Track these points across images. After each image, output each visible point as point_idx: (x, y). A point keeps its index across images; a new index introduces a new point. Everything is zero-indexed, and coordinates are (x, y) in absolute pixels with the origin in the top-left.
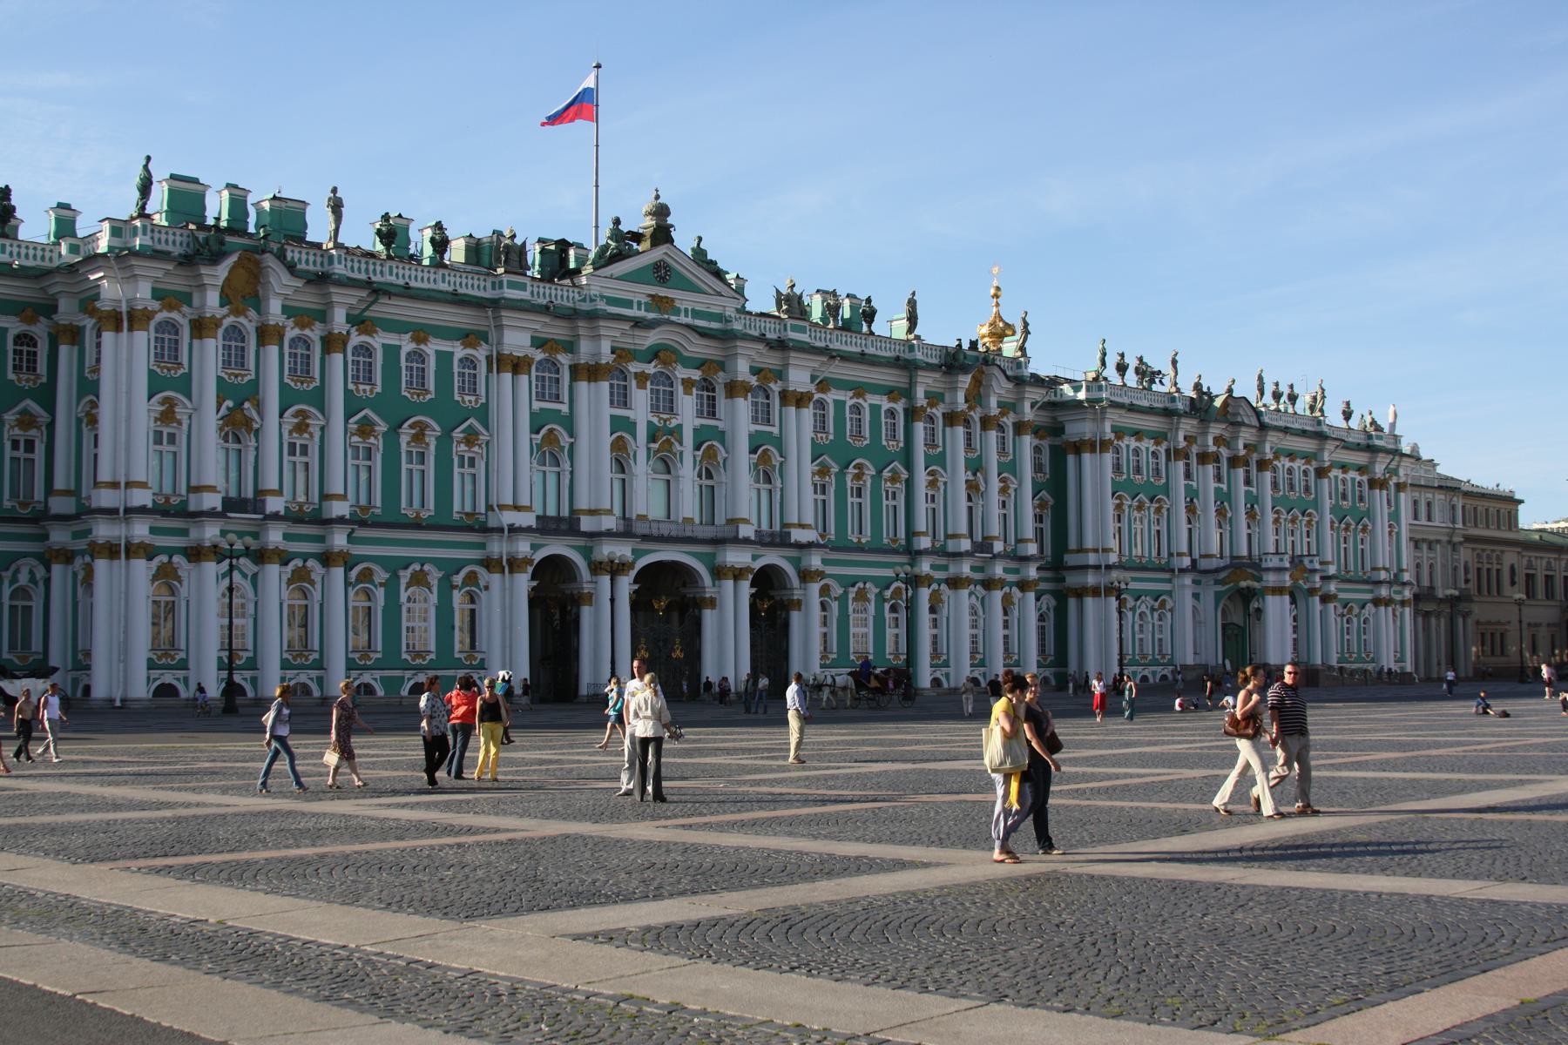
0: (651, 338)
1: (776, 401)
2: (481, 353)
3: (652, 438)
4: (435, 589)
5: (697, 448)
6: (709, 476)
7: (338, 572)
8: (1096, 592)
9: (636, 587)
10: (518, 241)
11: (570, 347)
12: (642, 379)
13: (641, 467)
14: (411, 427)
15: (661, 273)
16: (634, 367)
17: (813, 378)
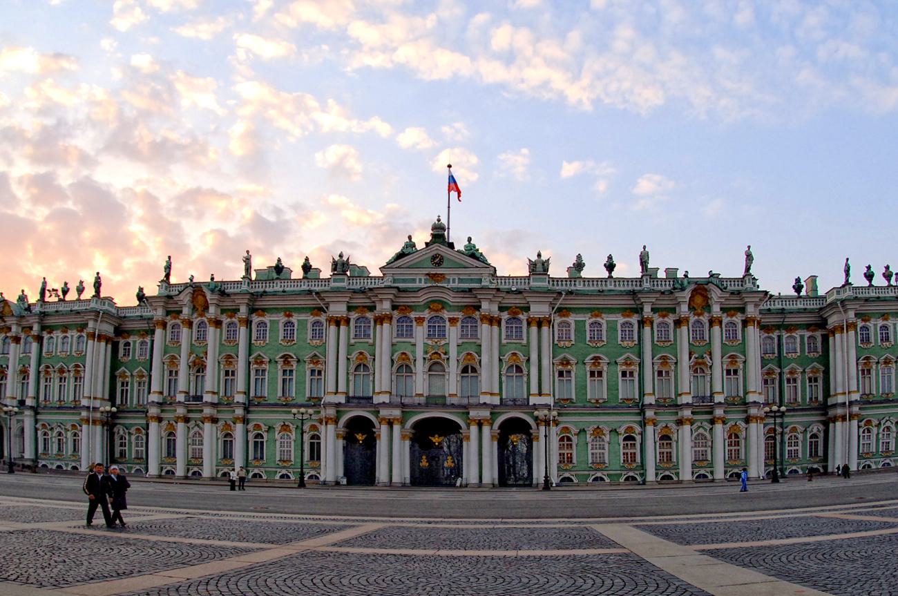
0: (422, 299)
1: (525, 323)
2: (323, 318)
3: (426, 352)
4: (294, 433)
5: (458, 356)
6: (474, 370)
7: (239, 427)
8: (843, 418)
9: (413, 431)
10: (345, 259)
11: (372, 308)
12: (420, 320)
13: (420, 368)
14: (281, 358)
15: (438, 260)
16: (413, 315)
17: (553, 308)
